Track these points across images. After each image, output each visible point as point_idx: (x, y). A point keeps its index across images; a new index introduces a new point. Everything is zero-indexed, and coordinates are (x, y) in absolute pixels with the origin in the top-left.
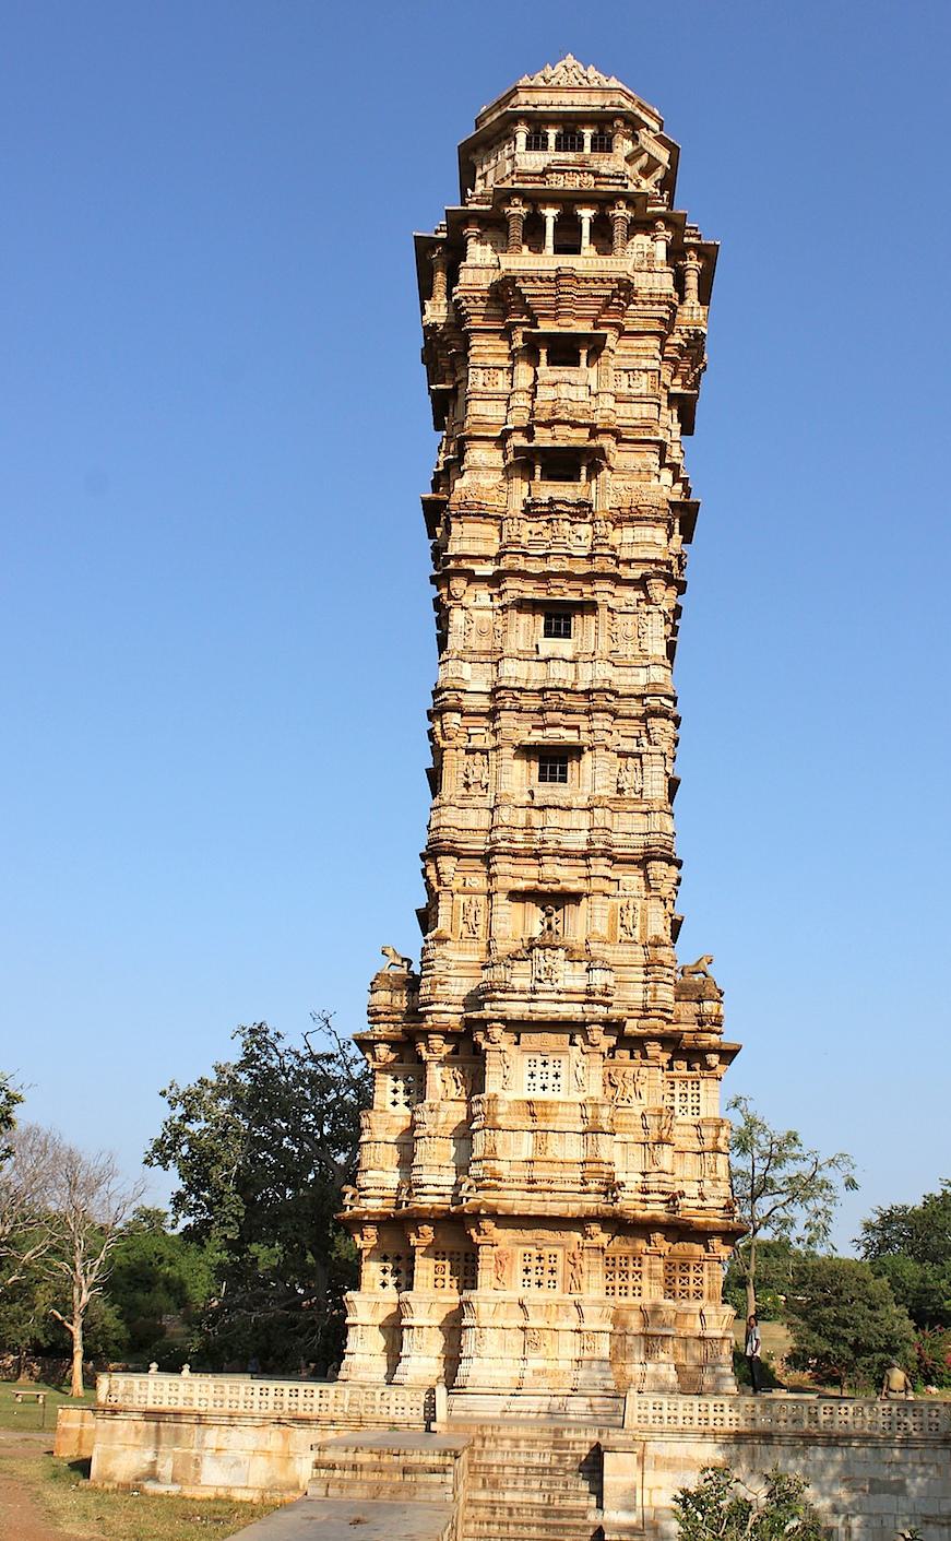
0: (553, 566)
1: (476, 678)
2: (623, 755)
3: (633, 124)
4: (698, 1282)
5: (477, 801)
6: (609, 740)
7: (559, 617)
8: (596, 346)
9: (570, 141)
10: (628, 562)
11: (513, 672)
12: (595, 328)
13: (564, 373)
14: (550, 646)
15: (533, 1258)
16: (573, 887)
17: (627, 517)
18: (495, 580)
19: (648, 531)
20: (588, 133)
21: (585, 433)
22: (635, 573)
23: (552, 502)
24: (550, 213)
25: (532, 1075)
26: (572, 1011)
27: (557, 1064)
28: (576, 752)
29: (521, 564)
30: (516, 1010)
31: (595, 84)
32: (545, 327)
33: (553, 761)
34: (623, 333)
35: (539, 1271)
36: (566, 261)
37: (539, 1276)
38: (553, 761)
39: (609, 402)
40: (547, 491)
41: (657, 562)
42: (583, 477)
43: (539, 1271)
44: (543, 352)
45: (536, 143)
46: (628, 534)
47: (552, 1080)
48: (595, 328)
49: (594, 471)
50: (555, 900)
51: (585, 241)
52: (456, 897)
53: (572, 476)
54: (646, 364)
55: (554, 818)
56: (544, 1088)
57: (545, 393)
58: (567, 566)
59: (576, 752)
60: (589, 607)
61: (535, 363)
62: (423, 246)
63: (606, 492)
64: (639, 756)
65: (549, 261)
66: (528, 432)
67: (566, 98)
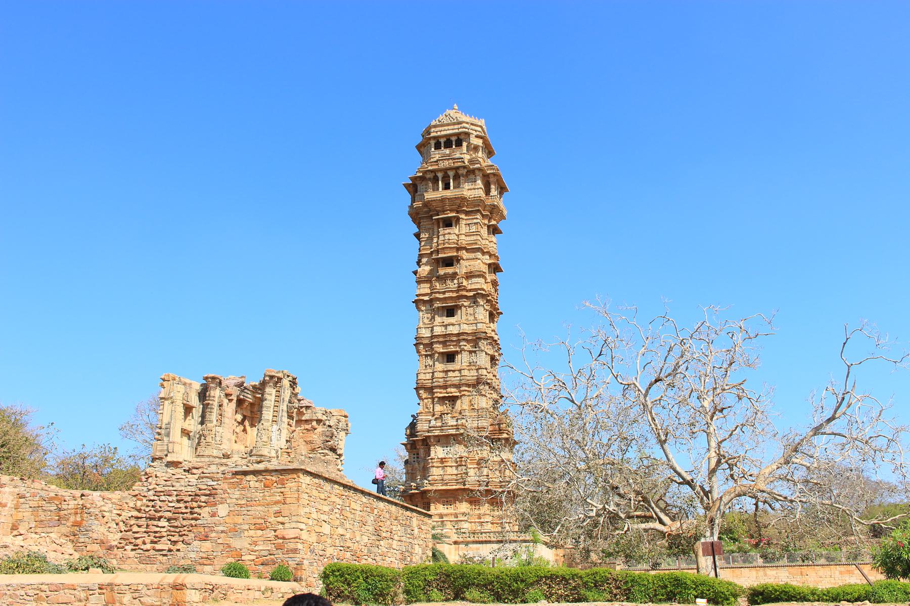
0: (447, 295)
1: (426, 333)
2: (470, 352)
3: (468, 134)
6: (466, 348)
7: (451, 312)
8: (458, 220)
9: (448, 144)
13: (447, 231)
16: (458, 394)
17: (469, 276)
18: (431, 302)
22: (471, 294)
23: (445, 274)
24: (440, 175)
28: (457, 353)
29: (438, 295)
30: (437, 433)
33: (450, 357)
34: (467, 213)
39: (463, 237)
45: (438, 146)
49: (458, 261)
51: (452, 184)
54: (475, 221)
55: (450, 374)
57: (441, 238)
58: (451, 294)
59: (457, 353)
61: (439, 227)
62: (407, 186)
63: (462, 268)
64: (475, 352)
67: (446, 128)
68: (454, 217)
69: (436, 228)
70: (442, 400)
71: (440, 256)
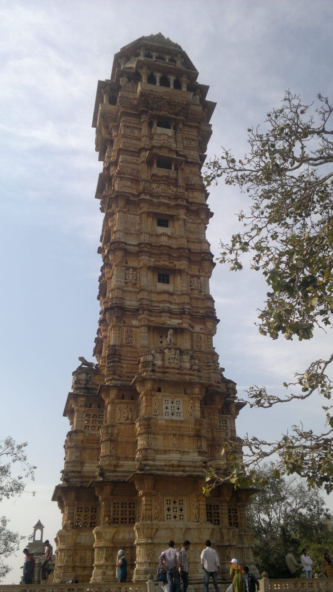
2: (193, 276)
4: (235, 518)
5: (130, 289)
14: (161, 230)
15: (172, 502)
35: (175, 510)
37: (174, 513)
43: (175, 510)
56: (173, 414)
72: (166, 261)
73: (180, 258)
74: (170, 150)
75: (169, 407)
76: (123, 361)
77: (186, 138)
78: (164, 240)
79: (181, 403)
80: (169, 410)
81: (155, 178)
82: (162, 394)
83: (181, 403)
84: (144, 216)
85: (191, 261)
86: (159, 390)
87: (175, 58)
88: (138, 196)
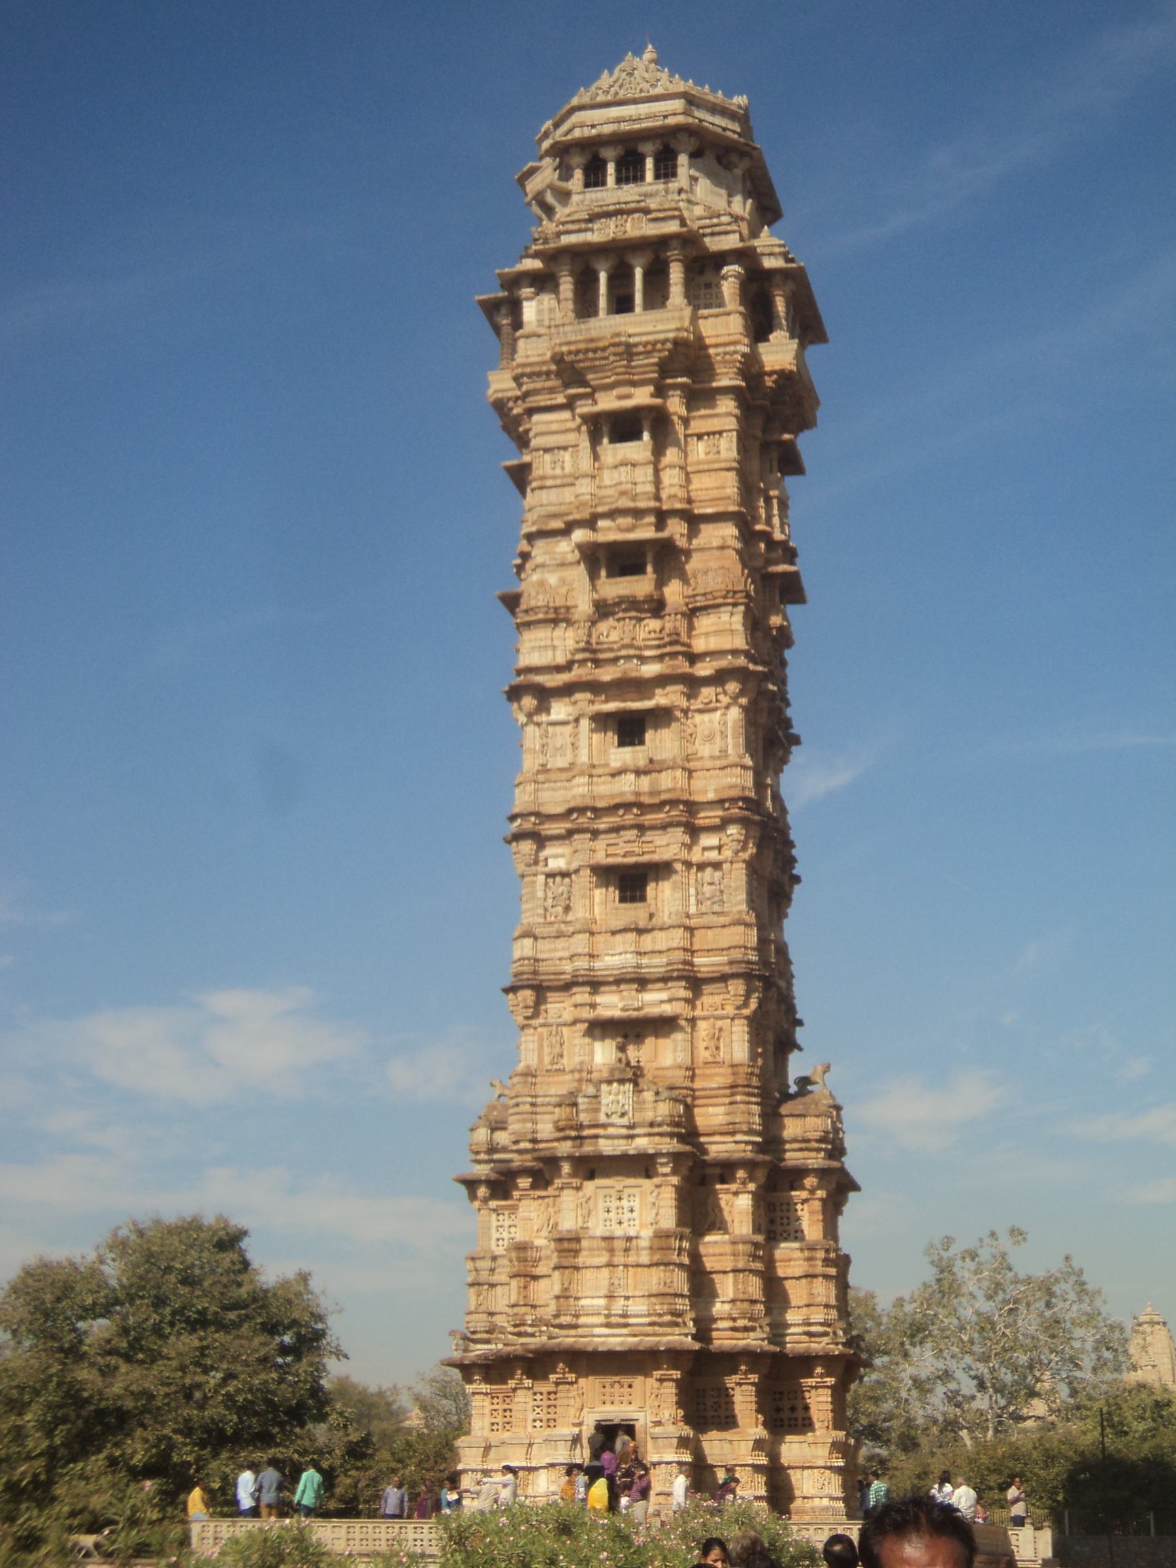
2: (701, 867)
9: (630, 171)
10: (701, 656)
11: (579, 790)
12: (652, 396)
19: (725, 617)
20: (648, 148)
21: (651, 519)
25: (608, 1211)
26: (642, 1144)
27: (632, 1198)
31: (659, 90)
32: (607, 402)
33: (631, 881)
36: (621, 323)
38: (631, 881)
40: (614, 588)
41: (735, 652)
42: (649, 569)
44: (605, 429)
46: (704, 623)
47: (628, 1215)
48: (655, 395)
50: (631, 1030)
52: (540, 1030)
53: (638, 570)
56: (620, 1223)
57: (608, 478)
60: (662, 717)
64: (717, 866)
65: (606, 325)
66: (590, 523)
68: (650, 409)
69: (585, 443)
70: (600, 1028)
71: (601, 538)
72: (634, 842)
73: (664, 827)
74: (638, 513)
75: (613, 1210)
76: (539, 1109)
77: (700, 437)
78: (627, 786)
79: (637, 1199)
80: (612, 1215)
81: (603, 610)
82: (599, 1182)
83: (637, 1199)
84: (585, 723)
85: (694, 831)
86: (591, 1176)
87: (673, 145)
88: (568, 667)
